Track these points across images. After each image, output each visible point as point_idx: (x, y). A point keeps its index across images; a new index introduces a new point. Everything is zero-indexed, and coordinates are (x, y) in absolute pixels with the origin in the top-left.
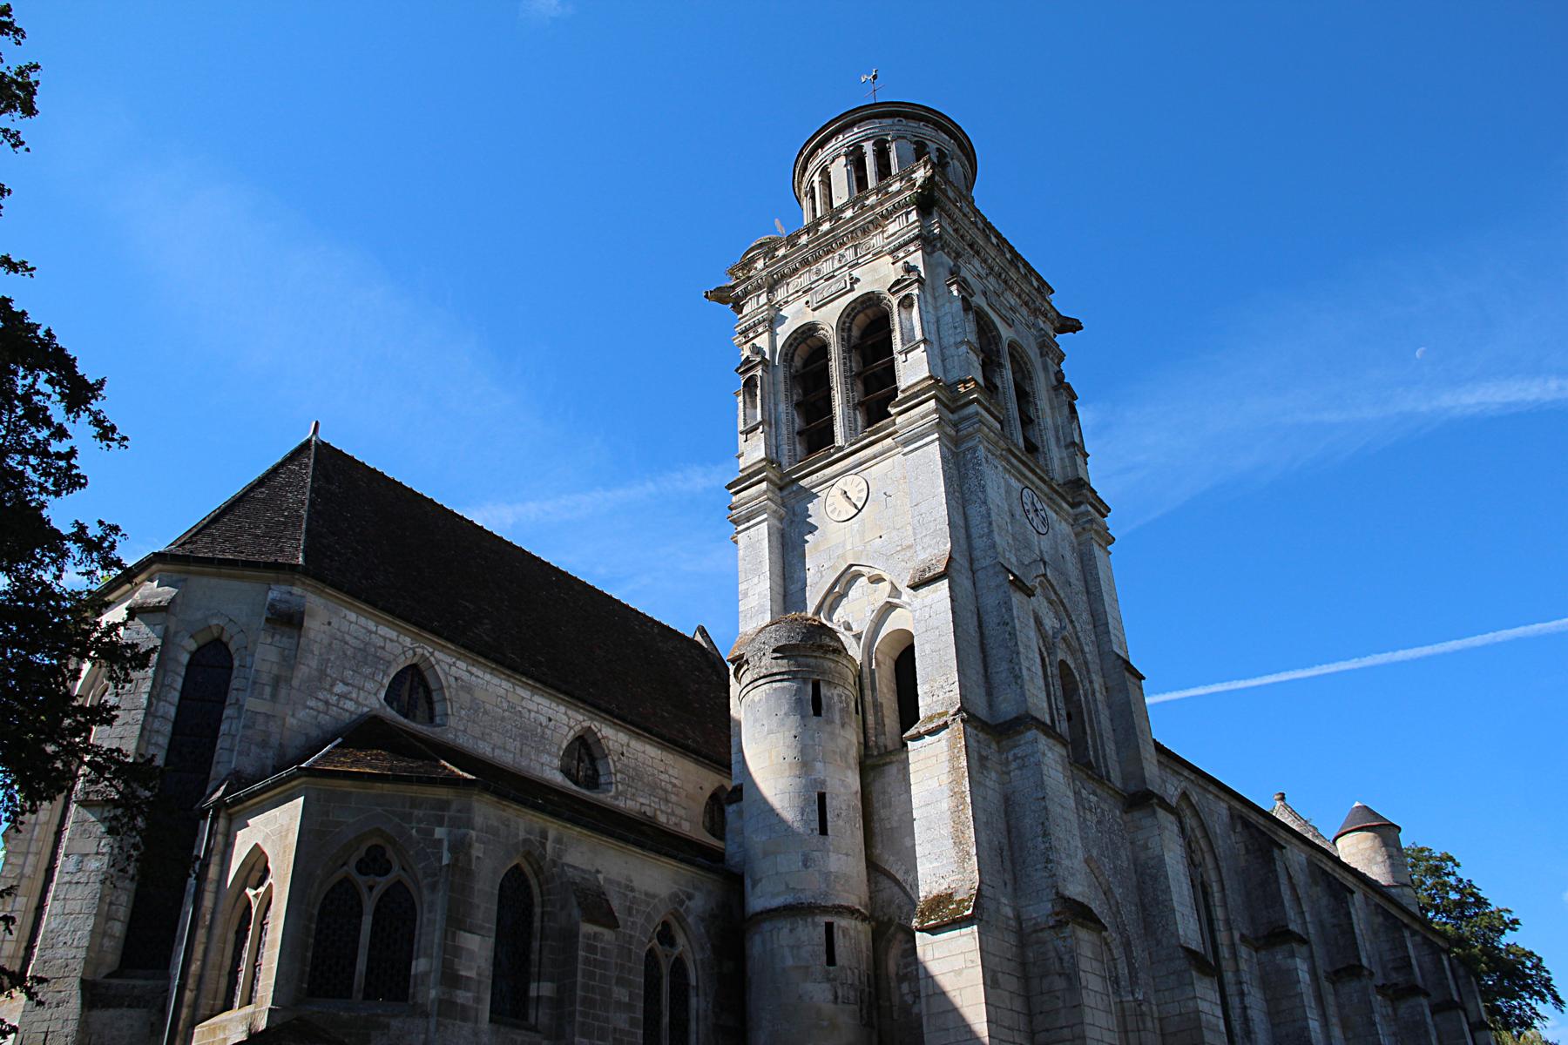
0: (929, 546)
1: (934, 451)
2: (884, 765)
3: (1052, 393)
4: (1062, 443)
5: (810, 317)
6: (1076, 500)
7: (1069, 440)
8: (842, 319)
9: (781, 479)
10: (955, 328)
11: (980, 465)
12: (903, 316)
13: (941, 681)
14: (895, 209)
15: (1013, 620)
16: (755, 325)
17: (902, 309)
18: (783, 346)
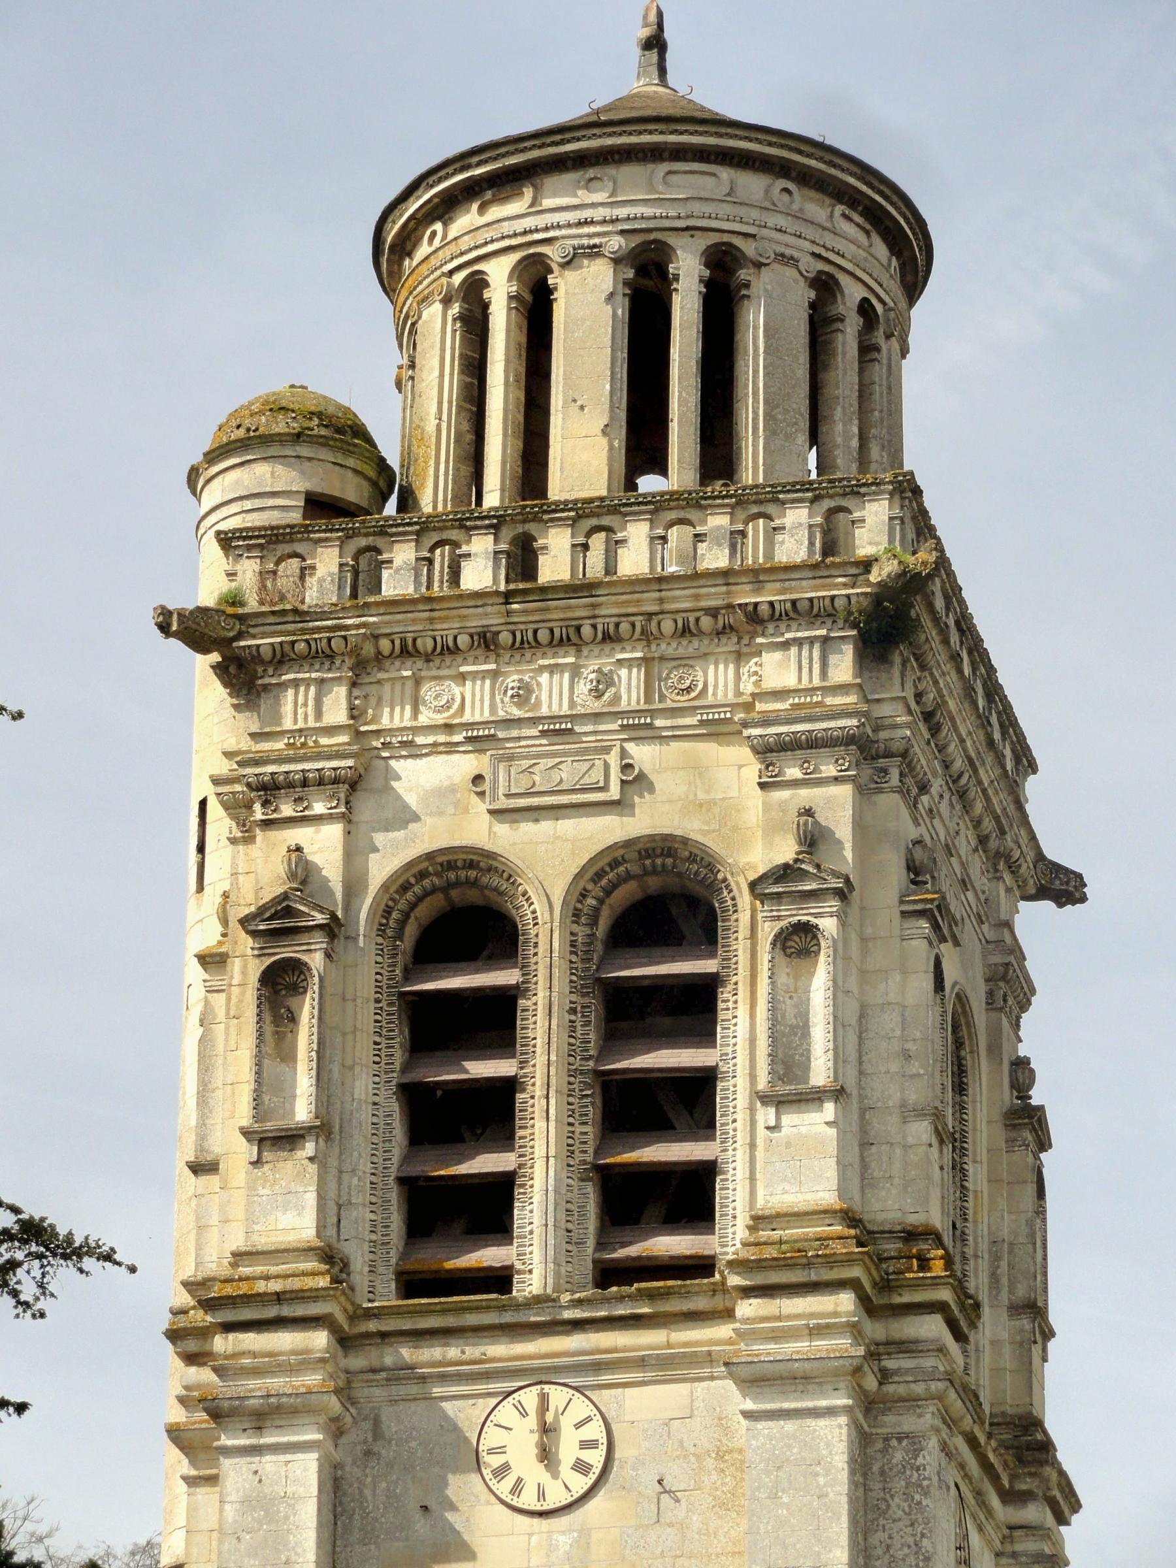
4: (1004, 1296)
6: (1022, 1486)
7: (1021, 1292)
8: (581, 885)
9: (352, 1318)
10: (907, 1056)
11: (926, 1494)
12: (782, 979)
14: (795, 613)
16: (305, 783)
17: (781, 959)
18: (385, 887)
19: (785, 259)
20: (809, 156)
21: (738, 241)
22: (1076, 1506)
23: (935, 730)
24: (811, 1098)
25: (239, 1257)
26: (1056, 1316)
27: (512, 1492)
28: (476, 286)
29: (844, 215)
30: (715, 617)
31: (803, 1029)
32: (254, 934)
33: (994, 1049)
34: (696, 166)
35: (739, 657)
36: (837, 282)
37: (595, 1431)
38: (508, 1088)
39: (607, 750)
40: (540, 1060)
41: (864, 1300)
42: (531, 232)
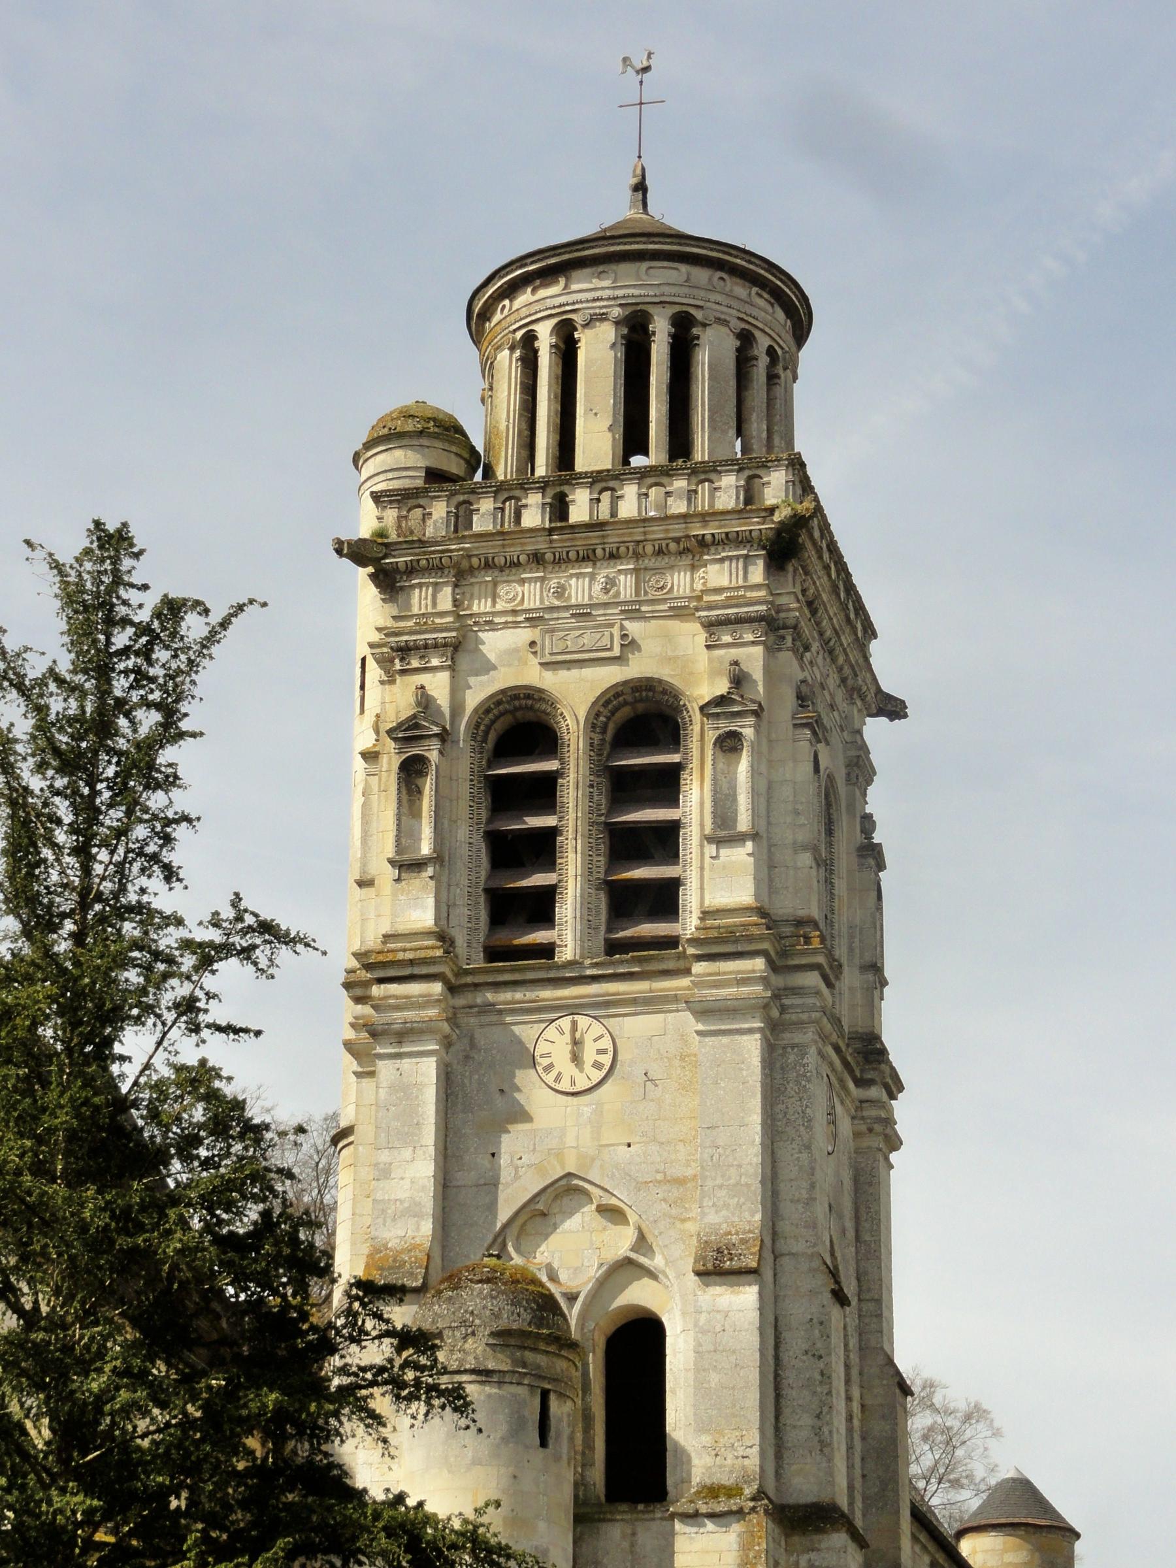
0: (726, 1206)
1: (751, 1047)
2: (604, 1520)
3: (855, 859)
4: (857, 961)
5: (533, 675)
6: (869, 1076)
7: (868, 958)
8: (596, 708)
10: (797, 813)
11: (809, 1081)
12: (720, 766)
13: (730, 1437)
14: (729, 540)
15: (829, 1354)
17: (720, 754)
18: (476, 710)
19: (720, 321)
20: (736, 257)
21: (692, 311)
22: (901, 1088)
23: (814, 612)
24: (740, 839)
25: (387, 937)
26: (888, 973)
27: (555, 1081)
28: (529, 339)
29: (757, 294)
30: (678, 543)
31: (733, 797)
32: (395, 739)
33: (851, 807)
34: (665, 264)
35: (693, 568)
36: (753, 335)
37: (606, 1043)
38: (551, 834)
39: (612, 625)
40: (571, 816)
41: (770, 963)
42: (564, 305)
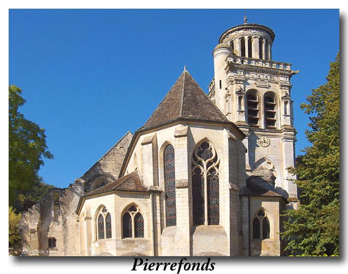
5: (255, 87)
